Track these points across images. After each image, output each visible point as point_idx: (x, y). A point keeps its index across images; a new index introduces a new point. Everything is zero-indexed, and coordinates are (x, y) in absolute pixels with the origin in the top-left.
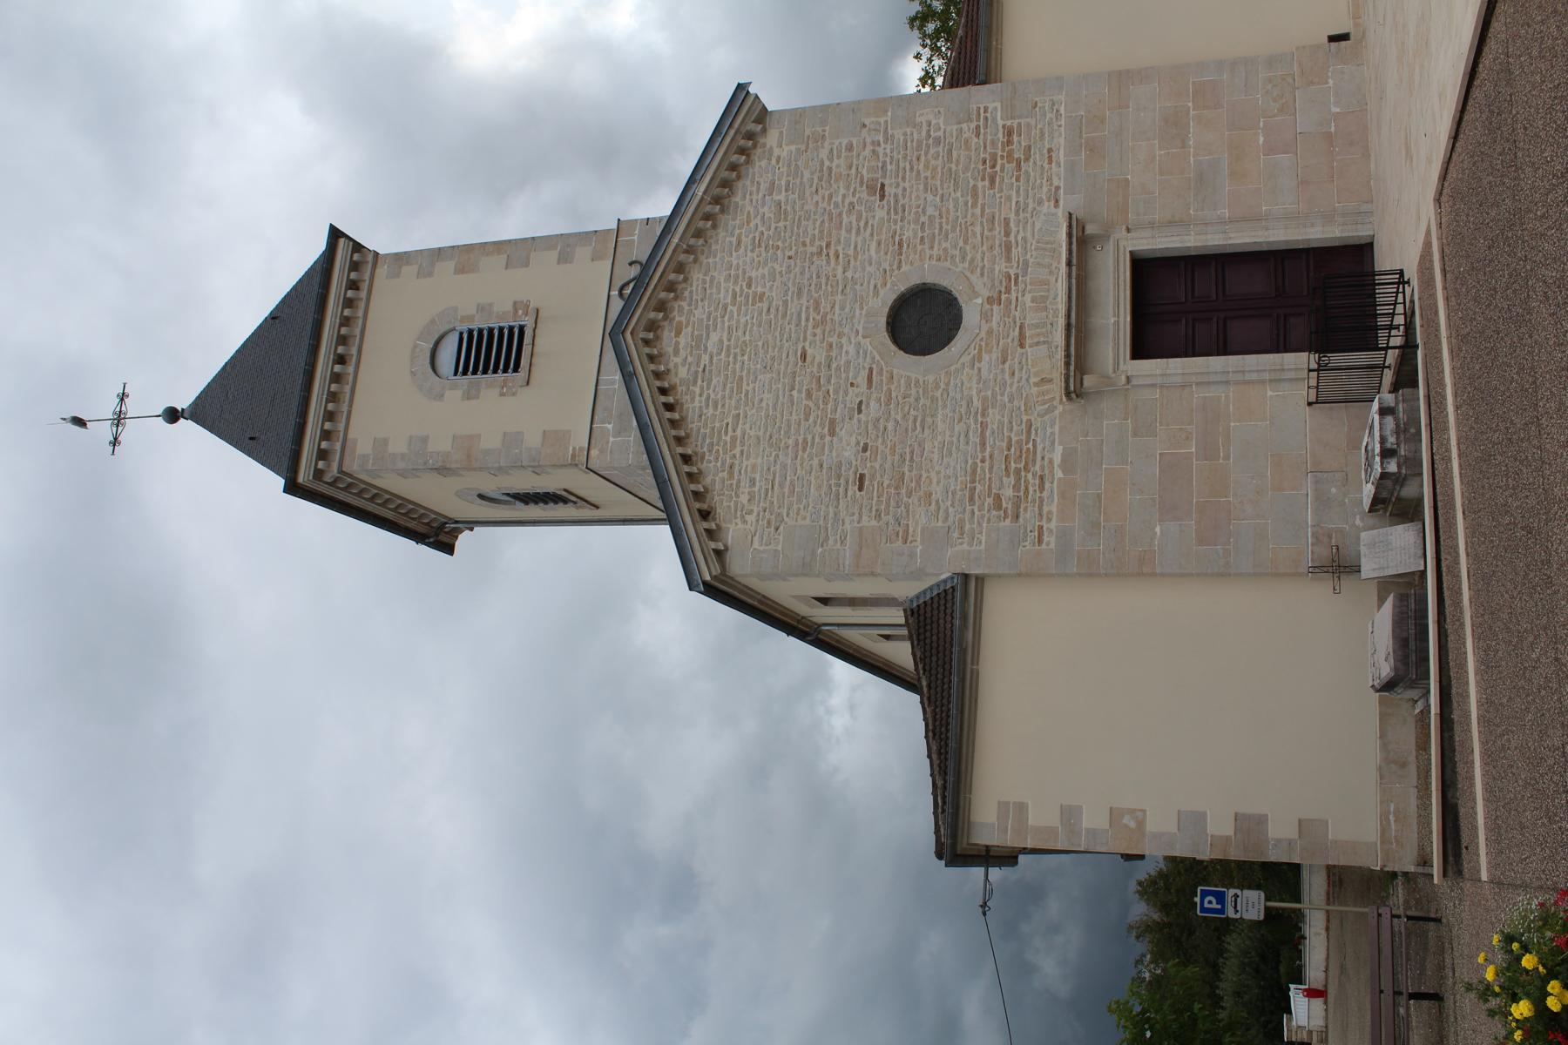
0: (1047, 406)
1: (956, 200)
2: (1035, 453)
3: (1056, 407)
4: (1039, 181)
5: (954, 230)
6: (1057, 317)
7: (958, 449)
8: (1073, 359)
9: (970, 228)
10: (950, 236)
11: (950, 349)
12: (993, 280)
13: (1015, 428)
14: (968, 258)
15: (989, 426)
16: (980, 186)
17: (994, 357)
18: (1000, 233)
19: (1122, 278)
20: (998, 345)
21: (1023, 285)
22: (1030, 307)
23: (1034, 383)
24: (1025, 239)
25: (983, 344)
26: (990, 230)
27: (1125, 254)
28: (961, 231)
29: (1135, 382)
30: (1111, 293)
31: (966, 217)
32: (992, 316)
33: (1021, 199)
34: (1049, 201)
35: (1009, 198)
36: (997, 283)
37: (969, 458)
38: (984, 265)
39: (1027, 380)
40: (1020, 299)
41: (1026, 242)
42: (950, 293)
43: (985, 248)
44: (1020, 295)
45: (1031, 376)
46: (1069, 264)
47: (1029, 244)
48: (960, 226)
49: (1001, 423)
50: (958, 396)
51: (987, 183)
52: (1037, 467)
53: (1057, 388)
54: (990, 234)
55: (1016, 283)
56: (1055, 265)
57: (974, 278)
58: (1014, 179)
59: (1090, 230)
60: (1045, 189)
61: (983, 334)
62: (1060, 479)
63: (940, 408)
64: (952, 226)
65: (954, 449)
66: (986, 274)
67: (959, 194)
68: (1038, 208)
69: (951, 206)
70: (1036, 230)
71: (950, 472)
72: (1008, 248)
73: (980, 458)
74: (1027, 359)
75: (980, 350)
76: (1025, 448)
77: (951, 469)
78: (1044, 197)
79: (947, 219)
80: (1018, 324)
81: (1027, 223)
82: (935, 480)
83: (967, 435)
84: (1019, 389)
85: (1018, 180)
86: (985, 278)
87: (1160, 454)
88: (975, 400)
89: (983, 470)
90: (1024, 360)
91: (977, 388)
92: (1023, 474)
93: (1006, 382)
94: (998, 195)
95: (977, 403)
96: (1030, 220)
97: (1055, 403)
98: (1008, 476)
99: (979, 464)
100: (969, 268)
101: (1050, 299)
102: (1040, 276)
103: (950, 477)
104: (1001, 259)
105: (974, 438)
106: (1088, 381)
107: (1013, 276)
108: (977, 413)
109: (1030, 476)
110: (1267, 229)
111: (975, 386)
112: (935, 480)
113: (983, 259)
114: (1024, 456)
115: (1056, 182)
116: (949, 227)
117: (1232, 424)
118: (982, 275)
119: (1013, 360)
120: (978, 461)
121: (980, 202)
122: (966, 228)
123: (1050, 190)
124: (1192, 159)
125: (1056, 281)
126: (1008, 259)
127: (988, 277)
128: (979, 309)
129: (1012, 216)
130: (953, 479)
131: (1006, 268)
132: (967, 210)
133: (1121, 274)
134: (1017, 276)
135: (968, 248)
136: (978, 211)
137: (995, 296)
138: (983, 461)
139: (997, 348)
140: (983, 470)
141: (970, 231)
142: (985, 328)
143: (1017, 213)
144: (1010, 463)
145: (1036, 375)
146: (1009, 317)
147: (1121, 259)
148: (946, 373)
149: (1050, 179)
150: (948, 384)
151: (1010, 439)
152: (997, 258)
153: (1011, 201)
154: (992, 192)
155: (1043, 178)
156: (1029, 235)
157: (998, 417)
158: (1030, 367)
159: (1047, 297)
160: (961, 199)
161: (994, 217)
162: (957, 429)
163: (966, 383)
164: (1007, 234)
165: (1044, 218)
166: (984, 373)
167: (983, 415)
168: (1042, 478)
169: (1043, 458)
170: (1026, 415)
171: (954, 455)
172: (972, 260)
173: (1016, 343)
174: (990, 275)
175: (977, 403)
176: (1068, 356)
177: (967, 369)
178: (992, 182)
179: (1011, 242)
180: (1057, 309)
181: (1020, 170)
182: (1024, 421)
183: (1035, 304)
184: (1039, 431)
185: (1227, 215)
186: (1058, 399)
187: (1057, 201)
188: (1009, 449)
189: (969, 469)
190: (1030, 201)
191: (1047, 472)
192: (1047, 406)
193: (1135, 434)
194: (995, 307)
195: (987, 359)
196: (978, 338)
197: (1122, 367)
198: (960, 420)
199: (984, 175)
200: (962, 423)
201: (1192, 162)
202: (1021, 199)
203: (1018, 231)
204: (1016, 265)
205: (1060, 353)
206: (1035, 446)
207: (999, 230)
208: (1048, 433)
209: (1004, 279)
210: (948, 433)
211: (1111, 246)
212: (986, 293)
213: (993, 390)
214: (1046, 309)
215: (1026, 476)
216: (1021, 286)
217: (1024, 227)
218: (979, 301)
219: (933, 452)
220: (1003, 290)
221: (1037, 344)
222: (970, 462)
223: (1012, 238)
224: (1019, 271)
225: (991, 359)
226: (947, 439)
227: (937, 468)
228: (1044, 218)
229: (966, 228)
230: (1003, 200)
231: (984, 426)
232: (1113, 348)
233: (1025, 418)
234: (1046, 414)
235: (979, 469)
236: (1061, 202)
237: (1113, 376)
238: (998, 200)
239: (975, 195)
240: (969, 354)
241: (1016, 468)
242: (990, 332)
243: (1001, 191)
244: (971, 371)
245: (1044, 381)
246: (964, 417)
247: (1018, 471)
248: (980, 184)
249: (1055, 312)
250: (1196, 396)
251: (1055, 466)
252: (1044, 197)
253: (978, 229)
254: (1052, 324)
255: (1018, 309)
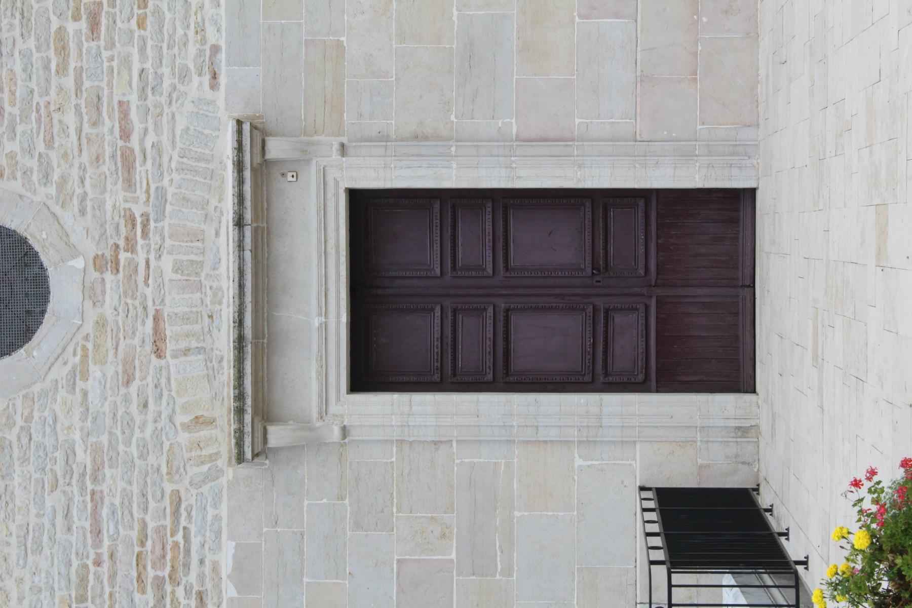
0: (205, 468)
1: (26, 56)
2: (188, 551)
3: (221, 471)
4: (180, 32)
5: (25, 118)
6: (220, 303)
7: (52, 539)
8: (249, 401)
9: (56, 117)
10: (19, 129)
11: (29, 354)
12: (102, 226)
13: (152, 505)
14: (56, 177)
15: (107, 500)
16: (71, 33)
17: (110, 372)
18: (112, 131)
19: (331, 243)
20: (117, 349)
21: (158, 238)
22: (171, 280)
23: (182, 425)
24: (157, 147)
25: (90, 346)
26: (95, 124)
27: (336, 194)
28: (39, 121)
29: (355, 435)
30: (315, 270)
31: (47, 93)
32: (104, 292)
33: (148, 65)
34: (200, 75)
35: (126, 62)
36: (110, 230)
37: (73, 556)
38: (85, 193)
39: (171, 419)
40: (153, 263)
41: (160, 154)
42: (23, 241)
43: (85, 159)
44: (152, 257)
45: (178, 410)
46: (239, 223)
47: (165, 159)
48: (38, 111)
49: (126, 496)
50: (49, 442)
51: (83, 25)
52: (193, 577)
53: (225, 444)
54: (94, 131)
55: (145, 234)
56: (214, 202)
57: (67, 217)
58: (134, 22)
59: (276, 149)
60: (192, 49)
61: (89, 327)
62: (231, 600)
63: (17, 463)
64: (22, 111)
65: (45, 538)
66: (89, 209)
67: (32, 43)
68: (180, 87)
69: (18, 68)
70: (178, 132)
71: (40, 580)
72: (128, 162)
73: (92, 556)
74: (169, 379)
75: (85, 356)
76: (170, 541)
77: (43, 575)
78: (191, 66)
79: (13, 93)
80: (151, 312)
81: (161, 114)
82: (14, 595)
83: (67, 515)
84: (157, 434)
85: (141, 25)
86: (89, 216)
87: (398, 561)
88: (79, 450)
89: (98, 578)
90: (163, 381)
91: (82, 430)
92: (168, 588)
93: (132, 419)
94: (105, 54)
95: (83, 457)
96: (166, 110)
97: (222, 463)
98: (143, 591)
99: (92, 568)
100: (58, 197)
101: (207, 270)
102: (189, 224)
103: (40, 591)
104: (116, 184)
105: (81, 521)
106: (277, 435)
107: (139, 220)
108: (83, 475)
109: (180, 592)
110: (580, 166)
111: (78, 424)
112: (14, 595)
113: (82, 181)
114: (168, 557)
115: (212, 36)
116: (16, 111)
117: (517, 514)
118: (83, 212)
119: (143, 378)
120: (90, 563)
121: (72, 64)
122: (49, 115)
123: (201, 52)
124: (455, 13)
125: (217, 234)
126: (130, 184)
127: (94, 216)
128: (79, 279)
129: (133, 99)
130: (45, 594)
131: (126, 201)
132: (48, 80)
133: (331, 234)
134: (146, 217)
135: (54, 156)
136: (69, 82)
137: (108, 254)
138: (98, 563)
139: (116, 353)
140: (98, 578)
141: (55, 121)
142: (92, 315)
143: (143, 96)
144: (145, 567)
145: (185, 408)
146: (134, 297)
147: (331, 205)
148: (25, 396)
149: (200, 30)
150: (29, 419)
151: (144, 525)
152: (109, 181)
153: (130, 69)
154: (93, 44)
155: (188, 26)
156: (165, 139)
157: (121, 485)
158: (174, 393)
159: (201, 264)
160: (36, 55)
161: (99, 98)
162: (49, 503)
163: (60, 415)
164: (126, 135)
165: (190, 107)
166: (94, 399)
167: (95, 480)
168: (201, 596)
169: (202, 562)
170: (170, 481)
171: (46, 551)
172: (64, 180)
173: (149, 347)
174: (98, 213)
175: (83, 457)
176: (240, 397)
177: (62, 393)
178: (94, 25)
179: (132, 151)
180: (220, 289)
181: (146, 7)
182: (168, 492)
183: (179, 277)
184: (193, 513)
185: (514, 131)
186: (225, 456)
187: (214, 76)
188: (142, 544)
189: (73, 576)
190: (166, 70)
191: (209, 585)
192: (205, 468)
193: (357, 525)
194: (109, 277)
195: (98, 374)
196: (80, 336)
197: (333, 408)
198: (54, 487)
199: (78, 9)
200: (58, 493)
201: (455, 18)
202: (148, 65)
203: (146, 131)
204: (143, 198)
205: (226, 371)
206: (186, 538)
207: (110, 124)
208: (209, 518)
209: (122, 222)
210: (33, 511)
211: (311, 176)
212: (91, 249)
213: (110, 433)
214: (200, 287)
215: (173, 592)
216: (154, 239)
217: (156, 124)
218: (79, 263)
219: (8, 544)
220: (122, 243)
221: (186, 352)
222: (75, 563)
223: (135, 143)
224: (150, 210)
225: (104, 375)
226: (33, 520)
227: (17, 573)
228: (190, 107)
229: (49, 115)
230: (115, 64)
231: (97, 499)
232: (319, 373)
233: (168, 488)
234: (204, 482)
235: (91, 577)
236: (223, 80)
237: (318, 424)
238: (106, 64)
239: (62, 50)
240: (65, 363)
241: (156, 578)
242: (101, 324)
243: (111, 45)
244: (70, 397)
245: (199, 422)
246: (61, 481)
247: (159, 583)
248: (71, 27)
249: (215, 295)
250: (457, 461)
251: (224, 576)
252: (191, 66)
253: (71, 119)
254: (211, 317)
255: (150, 282)
